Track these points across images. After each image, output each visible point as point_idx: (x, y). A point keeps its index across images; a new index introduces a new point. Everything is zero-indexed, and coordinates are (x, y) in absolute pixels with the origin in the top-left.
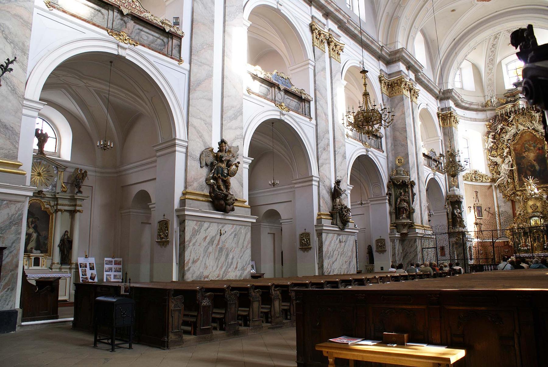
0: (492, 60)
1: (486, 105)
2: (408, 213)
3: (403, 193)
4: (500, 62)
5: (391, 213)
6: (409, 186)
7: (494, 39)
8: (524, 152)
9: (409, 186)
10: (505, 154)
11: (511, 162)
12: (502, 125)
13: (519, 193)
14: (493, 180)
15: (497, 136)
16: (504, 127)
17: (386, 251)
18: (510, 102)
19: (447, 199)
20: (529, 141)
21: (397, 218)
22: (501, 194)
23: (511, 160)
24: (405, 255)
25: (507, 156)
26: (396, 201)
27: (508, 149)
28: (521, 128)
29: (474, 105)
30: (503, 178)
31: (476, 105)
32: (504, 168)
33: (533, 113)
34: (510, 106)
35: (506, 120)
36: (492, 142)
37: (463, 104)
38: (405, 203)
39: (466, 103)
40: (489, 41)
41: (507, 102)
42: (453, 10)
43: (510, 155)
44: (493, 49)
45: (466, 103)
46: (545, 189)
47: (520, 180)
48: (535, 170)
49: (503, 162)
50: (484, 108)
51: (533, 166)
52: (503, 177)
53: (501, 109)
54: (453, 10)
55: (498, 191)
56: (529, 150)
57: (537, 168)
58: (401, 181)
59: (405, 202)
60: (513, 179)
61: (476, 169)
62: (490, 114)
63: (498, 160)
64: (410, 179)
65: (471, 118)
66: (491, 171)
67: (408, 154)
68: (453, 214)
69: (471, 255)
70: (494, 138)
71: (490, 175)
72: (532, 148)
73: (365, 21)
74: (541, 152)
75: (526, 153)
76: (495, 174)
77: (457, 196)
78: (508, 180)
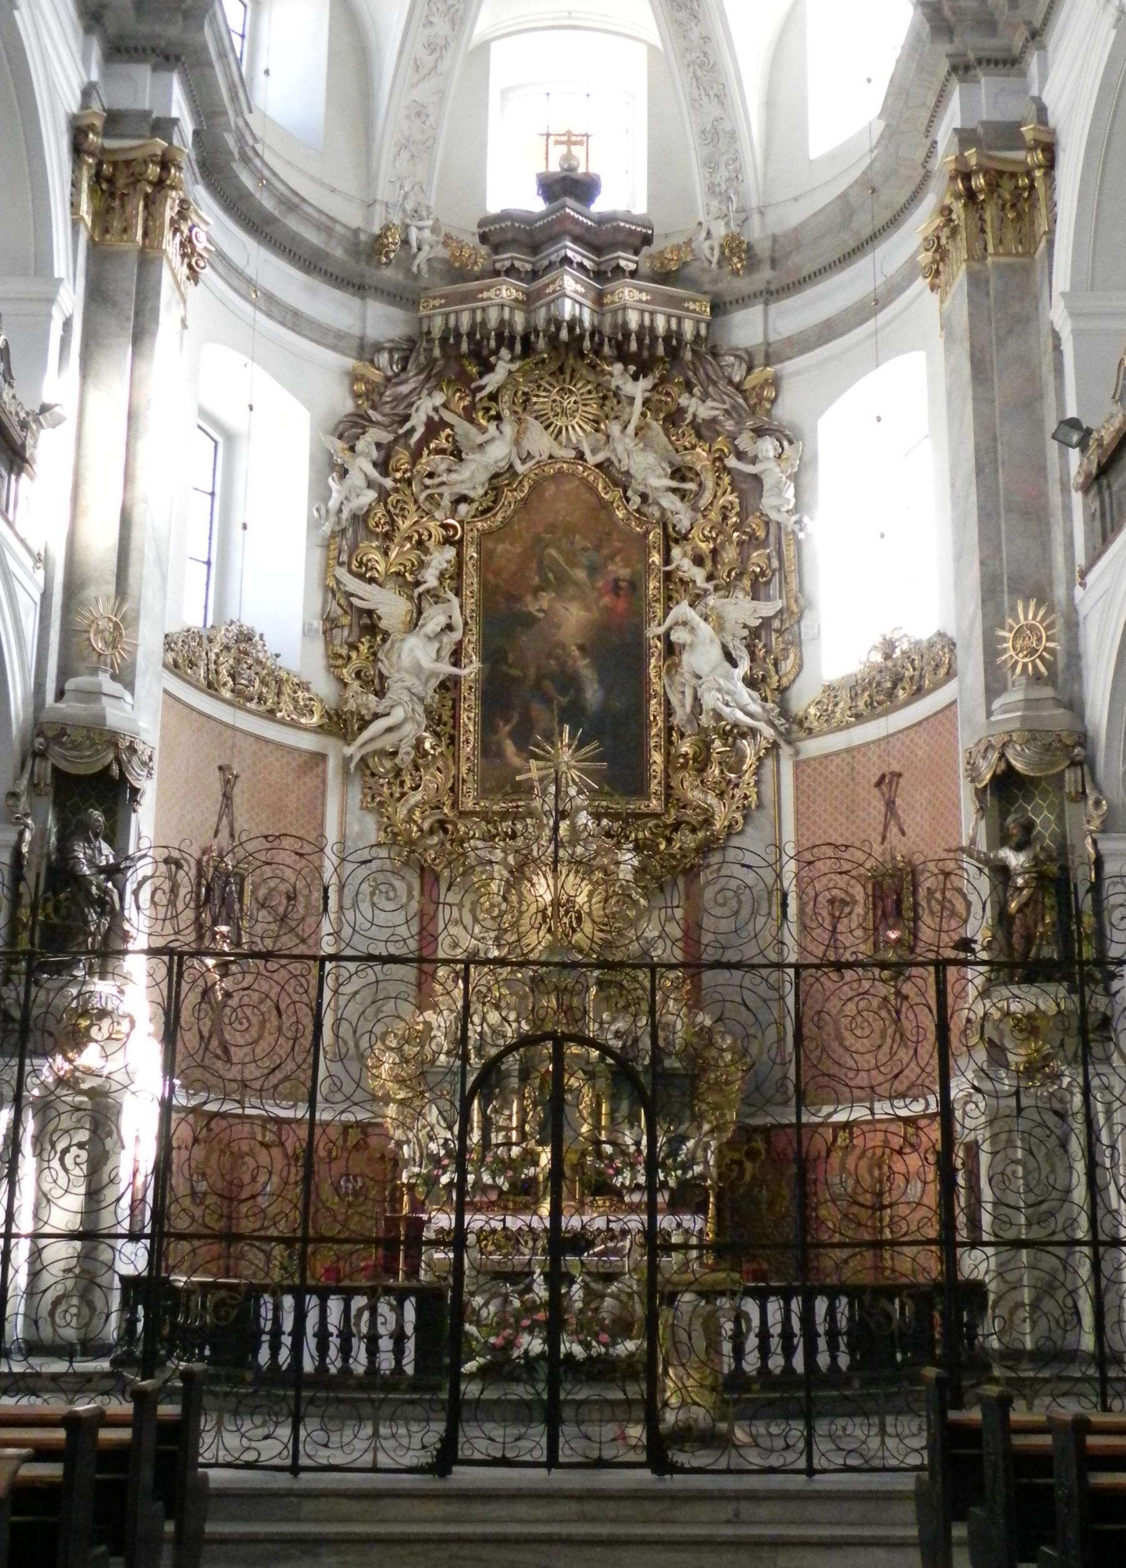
8: (536, 591)
10: (430, 578)
11: (457, 635)
12: (439, 399)
14: (341, 724)
15: (402, 457)
16: (448, 417)
20: (570, 530)
23: (458, 620)
25: (435, 597)
27: (450, 552)
29: (306, 219)
31: (319, 227)
32: (417, 657)
33: (618, 375)
34: (507, 291)
35: (463, 381)
36: (370, 484)
37: (246, 179)
43: (458, 592)
53: (450, 299)
55: (356, 794)
56: (560, 583)
57: (592, 694)
60: (452, 740)
61: (248, 622)
62: (383, 322)
63: (391, 606)
65: (270, 297)
66: (335, 661)
69: (974, 1223)
70: (383, 466)
71: (323, 686)
72: (581, 575)
74: (621, 605)
75: (545, 600)
76: (355, 685)
77: (112, 739)
78: (420, 741)
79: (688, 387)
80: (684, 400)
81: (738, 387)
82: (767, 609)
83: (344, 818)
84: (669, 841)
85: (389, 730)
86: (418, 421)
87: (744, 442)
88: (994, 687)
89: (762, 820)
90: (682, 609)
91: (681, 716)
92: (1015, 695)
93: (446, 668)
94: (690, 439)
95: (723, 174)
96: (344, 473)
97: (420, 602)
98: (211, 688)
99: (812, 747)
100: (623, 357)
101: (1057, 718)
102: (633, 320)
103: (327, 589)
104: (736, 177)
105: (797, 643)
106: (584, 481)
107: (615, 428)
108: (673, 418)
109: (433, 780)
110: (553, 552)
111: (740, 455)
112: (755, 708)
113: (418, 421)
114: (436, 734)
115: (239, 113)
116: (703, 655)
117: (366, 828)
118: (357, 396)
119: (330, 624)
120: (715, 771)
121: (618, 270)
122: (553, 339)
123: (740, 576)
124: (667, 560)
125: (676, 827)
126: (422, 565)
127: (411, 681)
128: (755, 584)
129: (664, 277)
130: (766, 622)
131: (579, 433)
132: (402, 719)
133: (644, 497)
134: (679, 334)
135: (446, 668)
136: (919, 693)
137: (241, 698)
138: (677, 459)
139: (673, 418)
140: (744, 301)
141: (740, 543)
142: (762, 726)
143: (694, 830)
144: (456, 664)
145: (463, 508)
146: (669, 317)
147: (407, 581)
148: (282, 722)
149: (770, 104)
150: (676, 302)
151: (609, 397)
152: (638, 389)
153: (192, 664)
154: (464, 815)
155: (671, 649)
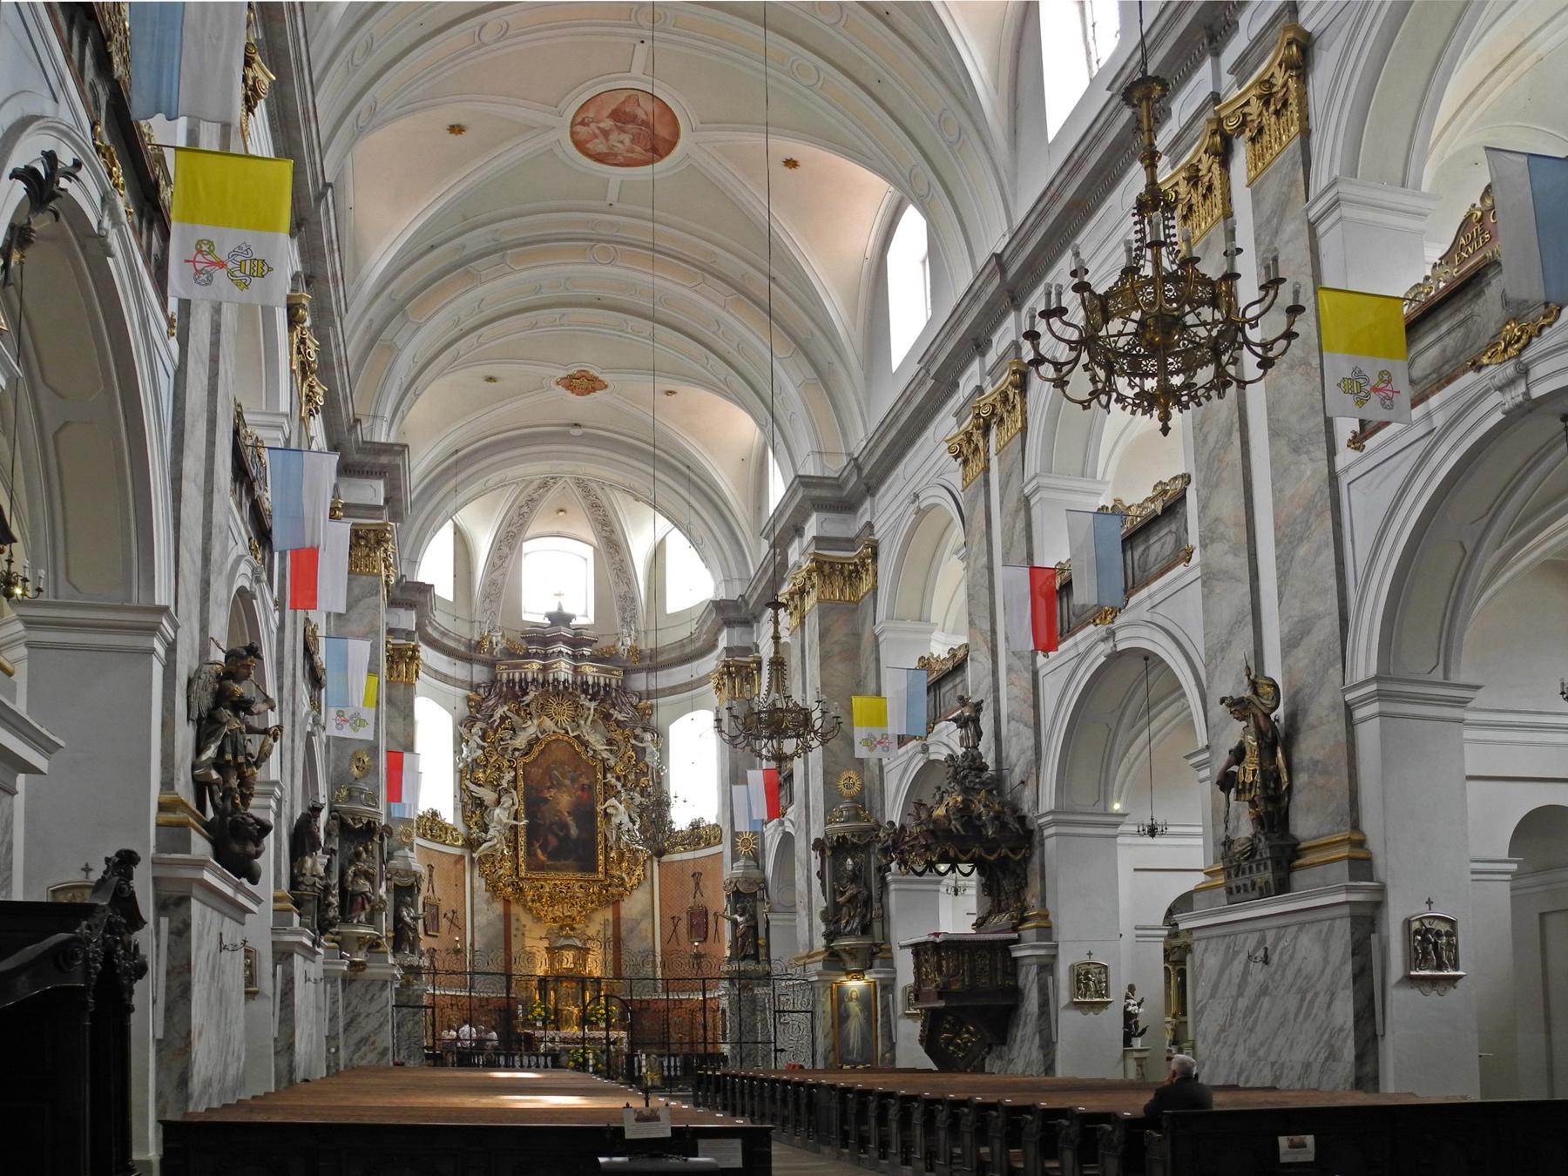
18: (536, 655)
24: (352, 1021)
25: (506, 791)
33: (583, 700)
34: (536, 665)
35: (516, 698)
41: (528, 655)
47: (530, 853)
48: (568, 835)
49: (498, 802)
50: (470, 653)
51: (565, 826)
53: (510, 667)
56: (559, 786)
57: (574, 831)
63: (488, 795)
72: (568, 782)
75: (553, 792)
81: (635, 707)
83: (475, 882)
86: (497, 716)
87: (638, 731)
88: (735, 858)
89: (647, 885)
91: (612, 841)
92: (741, 862)
95: (628, 615)
97: (500, 793)
99: (665, 858)
100: (585, 692)
101: (755, 873)
104: (634, 617)
108: (607, 717)
111: (636, 737)
113: (497, 716)
117: (480, 883)
120: (624, 865)
131: (564, 719)
132: (495, 838)
136: (708, 845)
144: (515, 819)
147: (495, 785)
149: (648, 588)
151: (577, 706)
152: (593, 705)
155: (607, 815)
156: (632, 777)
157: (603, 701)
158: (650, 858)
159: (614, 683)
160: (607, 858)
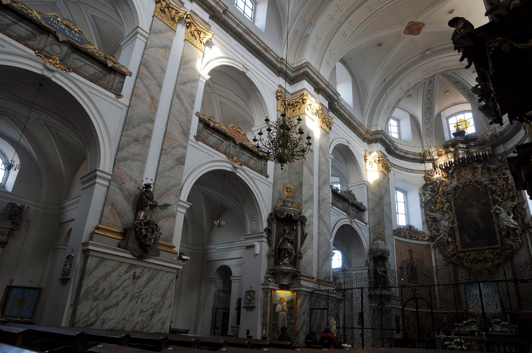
0: (430, 109)
1: (424, 155)
2: (293, 258)
3: (287, 231)
4: (439, 115)
5: (269, 256)
6: (299, 223)
7: (430, 84)
9: (299, 223)
11: (452, 219)
13: (462, 255)
14: (432, 238)
17: (254, 307)
19: (370, 254)
21: (276, 263)
22: (441, 255)
26: (278, 240)
28: (463, 181)
29: (410, 154)
30: (442, 235)
31: (413, 155)
37: (397, 152)
38: (289, 244)
39: (401, 151)
40: (424, 86)
42: (380, 45)
43: (451, 211)
44: (429, 96)
45: (401, 151)
46: (491, 251)
47: (461, 239)
52: (443, 235)
54: (380, 45)
55: (437, 251)
57: (482, 225)
58: (285, 214)
59: (289, 242)
60: (455, 238)
63: (438, 215)
64: (300, 213)
67: (302, 183)
68: (376, 272)
70: (433, 191)
71: (427, 232)
72: (475, 203)
73: (264, 32)
77: (381, 250)
78: (448, 240)
79: (490, 163)
80: (490, 166)
82: (515, 203)
84: (504, 253)
85: (441, 238)
87: (504, 171)
90: (497, 206)
93: (450, 225)
94: (493, 173)
96: (425, 194)
98: (405, 237)
100: (476, 161)
102: (475, 154)
103: (425, 215)
105: (524, 210)
106: (473, 185)
107: (476, 174)
108: (489, 169)
109: (452, 247)
110: (469, 200)
112: (515, 224)
114: (451, 238)
115: (392, 144)
116: (503, 215)
118: (425, 180)
119: (427, 221)
121: (471, 146)
122: (459, 162)
123: (508, 198)
124: (493, 197)
125: (505, 249)
126: (443, 207)
127: (443, 229)
128: (512, 198)
129: (481, 145)
130: (516, 206)
131: (469, 176)
133: (485, 186)
134: (485, 154)
135: (450, 225)
137: (411, 238)
138: (491, 177)
139: (489, 169)
140: (498, 145)
141: (508, 191)
142: (518, 227)
143: (509, 250)
145: (450, 195)
146: (482, 152)
147: (441, 210)
148: (420, 240)
150: (484, 149)
152: (479, 166)
153: (400, 234)
154: (460, 252)
156: (506, 193)
157: (485, 163)
158: (523, 232)
159: (487, 153)
160: (501, 236)
